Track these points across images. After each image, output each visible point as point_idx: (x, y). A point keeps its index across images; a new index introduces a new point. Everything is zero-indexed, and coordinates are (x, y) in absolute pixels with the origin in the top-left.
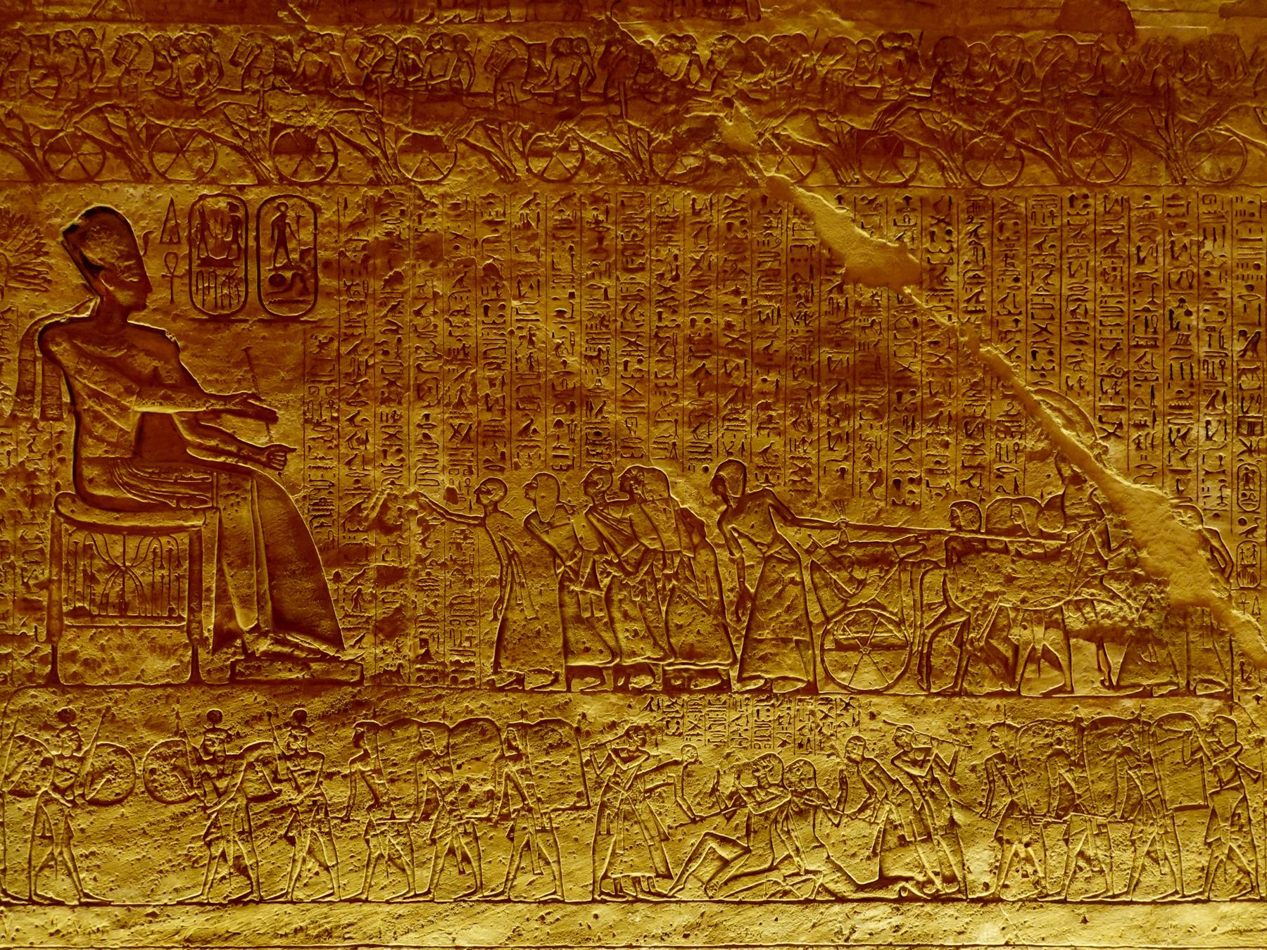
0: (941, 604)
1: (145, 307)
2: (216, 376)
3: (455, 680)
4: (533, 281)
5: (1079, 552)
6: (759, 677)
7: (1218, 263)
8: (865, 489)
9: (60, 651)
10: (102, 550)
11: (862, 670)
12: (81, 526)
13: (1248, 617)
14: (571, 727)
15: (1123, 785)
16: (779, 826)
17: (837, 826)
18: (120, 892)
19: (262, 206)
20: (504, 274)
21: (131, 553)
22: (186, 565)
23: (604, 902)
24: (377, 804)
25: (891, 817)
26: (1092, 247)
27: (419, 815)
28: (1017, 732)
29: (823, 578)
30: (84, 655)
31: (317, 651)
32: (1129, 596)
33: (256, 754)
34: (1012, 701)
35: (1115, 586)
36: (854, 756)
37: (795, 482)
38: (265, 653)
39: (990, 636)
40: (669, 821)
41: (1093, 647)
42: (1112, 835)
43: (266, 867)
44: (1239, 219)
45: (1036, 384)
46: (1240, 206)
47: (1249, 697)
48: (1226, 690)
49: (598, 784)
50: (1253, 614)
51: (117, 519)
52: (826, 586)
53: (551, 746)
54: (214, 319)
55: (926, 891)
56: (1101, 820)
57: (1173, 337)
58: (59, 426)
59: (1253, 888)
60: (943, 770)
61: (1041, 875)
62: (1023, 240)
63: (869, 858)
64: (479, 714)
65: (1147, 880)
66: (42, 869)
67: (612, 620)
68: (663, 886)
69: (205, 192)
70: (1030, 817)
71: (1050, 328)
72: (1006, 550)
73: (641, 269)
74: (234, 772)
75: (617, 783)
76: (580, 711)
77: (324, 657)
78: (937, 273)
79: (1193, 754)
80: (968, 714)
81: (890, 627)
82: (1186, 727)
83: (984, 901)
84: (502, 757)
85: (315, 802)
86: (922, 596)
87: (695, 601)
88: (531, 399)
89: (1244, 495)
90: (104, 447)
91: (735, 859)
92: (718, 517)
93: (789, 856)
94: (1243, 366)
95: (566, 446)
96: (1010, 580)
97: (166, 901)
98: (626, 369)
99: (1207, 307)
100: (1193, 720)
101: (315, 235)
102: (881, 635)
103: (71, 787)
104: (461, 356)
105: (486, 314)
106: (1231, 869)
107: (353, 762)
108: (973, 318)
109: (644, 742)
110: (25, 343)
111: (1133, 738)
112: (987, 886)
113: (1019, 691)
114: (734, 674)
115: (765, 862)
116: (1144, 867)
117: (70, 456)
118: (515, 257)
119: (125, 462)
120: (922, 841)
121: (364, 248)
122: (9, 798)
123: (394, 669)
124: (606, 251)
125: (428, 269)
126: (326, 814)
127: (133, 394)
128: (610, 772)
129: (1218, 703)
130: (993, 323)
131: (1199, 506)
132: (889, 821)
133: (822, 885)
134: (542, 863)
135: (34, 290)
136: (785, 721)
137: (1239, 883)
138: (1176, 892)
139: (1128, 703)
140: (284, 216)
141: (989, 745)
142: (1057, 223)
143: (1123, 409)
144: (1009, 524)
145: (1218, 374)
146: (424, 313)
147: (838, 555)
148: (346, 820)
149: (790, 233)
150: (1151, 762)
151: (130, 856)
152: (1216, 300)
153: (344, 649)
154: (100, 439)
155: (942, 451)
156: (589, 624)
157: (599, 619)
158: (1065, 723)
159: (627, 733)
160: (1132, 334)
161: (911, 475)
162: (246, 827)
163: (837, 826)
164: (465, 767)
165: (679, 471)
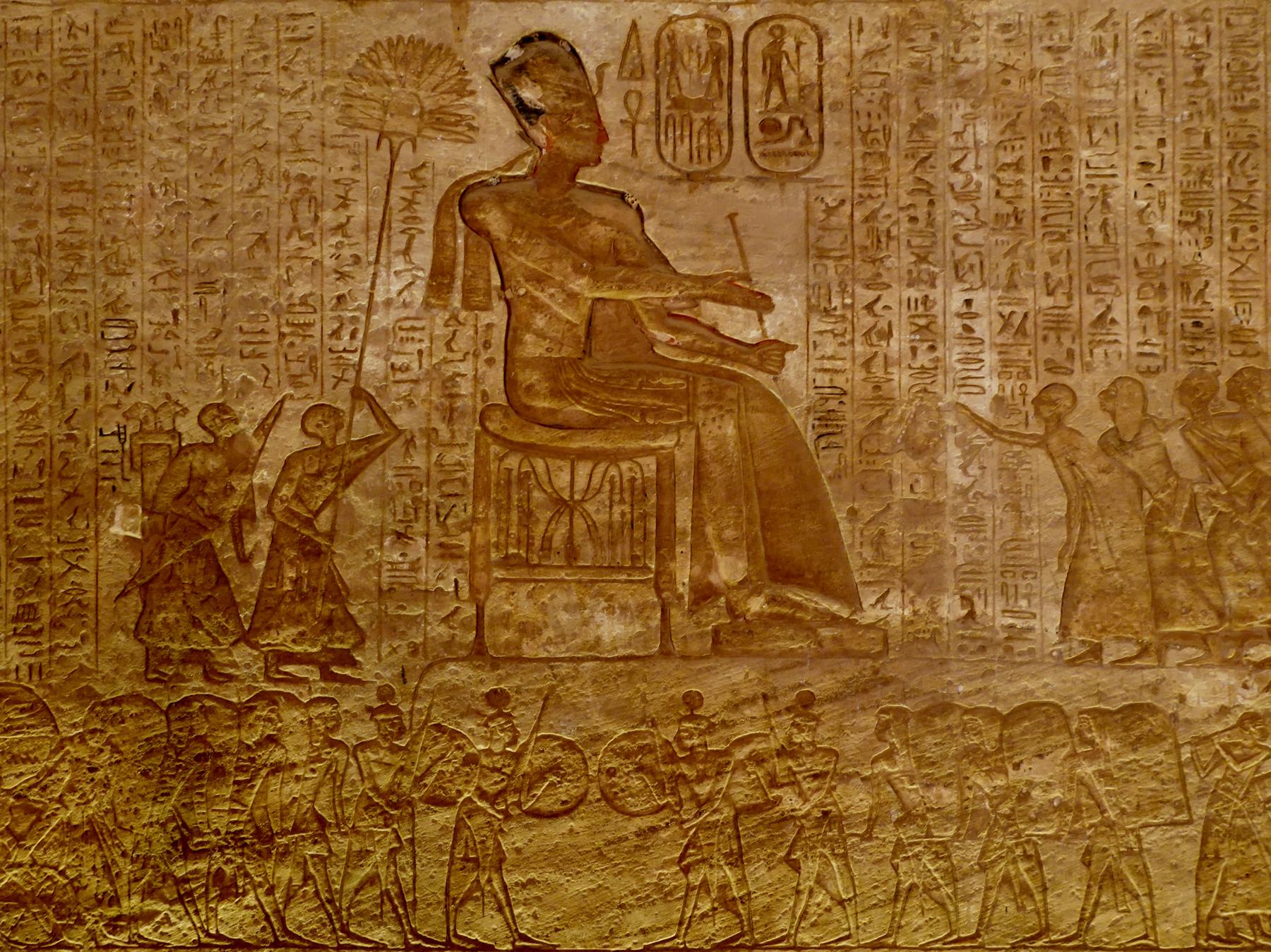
1: (599, 161)
2: (692, 250)
3: (1009, 650)
4: (1110, 124)
9: (487, 612)
10: (544, 478)
12: (514, 447)
18: (568, 933)
19: (751, 28)
20: (1072, 115)
21: (581, 483)
22: (653, 499)
24: (908, 817)
27: (963, 832)
30: (519, 617)
31: (826, 613)
33: (747, 750)
38: (760, 615)
43: (760, 901)
51: (563, 438)
53: (1139, 739)
54: (689, 177)
58: (485, 318)
64: (1041, 696)
66: (463, 902)
67: (1217, 572)
69: (678, 11)
74: (719, 773)
75: (1227, 790)
76: (1176, 692)
77: (835, 620)
84: (1074, 755)
85: (826, 814)
88: (1105, 280)
90: (546, 344)
95: (1154, 341)
97: (629, 945)
98: (1234, 238)
101: (820, 70)
103: (502, 792)
104: (1012, 223)
107: (874, 761)
110: (441, 210)
117: (500, 357)
118: (1085, 94)
119: (574, 363)
121: (883, 84)
122: (421, 806)
123: (927, 636)
124: (1206, 84)
125: (969, 110)
126: (841, 831)
127: (584, 274)
135: (457, 141)
140: (777, 43)
146: (963, 167)
148: (867, 836)
151: (581, 886)
153: (862, 610)
154: (541, 335)
156: (1189, 576)
157: (1204, 569)
159: (1241, 723)
162: (735, 847)
164: (1024, 766)
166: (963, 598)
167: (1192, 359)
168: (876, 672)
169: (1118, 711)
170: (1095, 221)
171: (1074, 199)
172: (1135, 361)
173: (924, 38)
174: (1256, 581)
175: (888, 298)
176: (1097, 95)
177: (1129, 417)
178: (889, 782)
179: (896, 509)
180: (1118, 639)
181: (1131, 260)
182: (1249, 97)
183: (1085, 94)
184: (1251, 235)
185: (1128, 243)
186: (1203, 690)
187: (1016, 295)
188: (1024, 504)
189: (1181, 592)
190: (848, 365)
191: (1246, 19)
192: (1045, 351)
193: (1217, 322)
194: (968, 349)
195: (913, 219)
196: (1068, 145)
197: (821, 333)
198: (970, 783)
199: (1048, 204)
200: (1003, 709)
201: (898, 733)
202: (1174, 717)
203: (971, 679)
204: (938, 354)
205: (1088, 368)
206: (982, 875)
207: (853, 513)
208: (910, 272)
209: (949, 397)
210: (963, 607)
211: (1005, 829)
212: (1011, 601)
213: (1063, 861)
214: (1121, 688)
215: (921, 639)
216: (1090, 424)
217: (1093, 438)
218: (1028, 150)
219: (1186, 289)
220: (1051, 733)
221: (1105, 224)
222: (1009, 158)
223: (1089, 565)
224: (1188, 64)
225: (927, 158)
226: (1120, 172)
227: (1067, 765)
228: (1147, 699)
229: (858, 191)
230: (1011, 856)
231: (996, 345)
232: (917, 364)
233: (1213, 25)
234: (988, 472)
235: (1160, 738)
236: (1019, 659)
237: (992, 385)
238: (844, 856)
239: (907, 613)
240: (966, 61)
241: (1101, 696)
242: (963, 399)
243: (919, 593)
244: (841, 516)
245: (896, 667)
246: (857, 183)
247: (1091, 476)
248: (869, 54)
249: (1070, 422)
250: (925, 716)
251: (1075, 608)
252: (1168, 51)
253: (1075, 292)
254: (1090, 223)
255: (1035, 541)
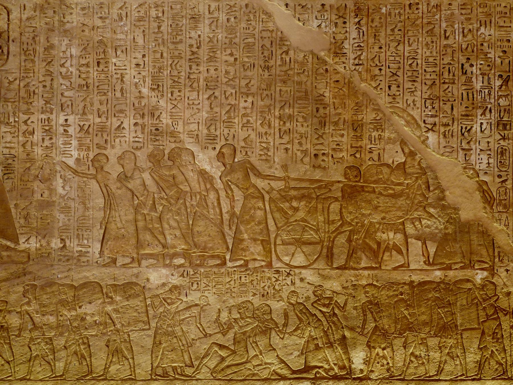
0: (339, 220)
3: (79, 260)
4: (124, 48)
5: (413, 193)
6: (241, 259)
7: (487, 38)
8: (299, 159)
11: (296, 255)
13: (502, 227)
14: (141, 286)
15: (435, 317)
16: (251, 339)
17: (282, 339)
20: (109, 45)
23: (156, 380)
25: (312, 334)
26: (421, 31)
27: (58, 333)
28: (379, 289)
29: (276, 207)
32: (439, 216)
34: (376, 272)
35: (432, 210)
36: (292, 302)
37: (261, 155)
39: (365, 237)
40: (193, 336)
41: (420, 243)
42: (429, 344)
44: (499, 16)
45: (391, 103)
46: (499, 9)
47: (502, 270)
48: (490, 266)
49: (155, 317)
50: (505, 225)
52: (277, 211)
53: (130, 296)
55: (330, 374)
56: (423, 336)
57: (463, 78)
59: (504, 373)
60: (340, 310)
61: (391, 365)
62: (384, 27)
63: (299, 356)
65: (448, 368)
68: (189, 371)
70: (385, 334)
71: (398, 73)
72: (374, 192)
73: (181, 42)
75: (165, 316)
76: (145, 277)
77: (8, 248)
78: (338, 44)
79: (472, 300)
80: (353, 279)
81: (312, 232)
82: (469, 285)
83: (360, 379)
84: (104, 302)
86: (329, 216)
87: (207, 218)
88: (121, 111)
89: (501, 162)
91: (228, 356)
92: (220, 174)
93: (257, 355)
94: (500, 93)
95: (140, 136)
96: (376, 208)
99: (482, 62)
100: (472, 282)
101: (8, 24)
102: (306, 236)
104: (85, 88)
105: (98, 66)
106: (493, 363)
107: (23, 305)
108: (357, 67)
109: (180, 293)
111: (441, 292)
112: (362, 371)
113: (380, 266)
114: (228, 257)
115: (244, 358)
116: (446, 362)
118: (115, 36)
120: (328, 347)
123: (46, 255)
124: (162, 32)
125: (68, 42)
128: (161, 310)
129: (485, 273)
130: (368, 71)
131: (477, 167)
132: (310, 336)
133: (274, 371)
134: (124, 359)
136: (255, 283)
137: (497, 369)
138: (463, 375)
139: (438, 273)
141: (364, 295)
142: (402, 18)
143: (436, 116)
144: (376, 178)
145: (487, 98)
146: (66, 65)
147: (284, 194)
148: (19, 336)
149: (261, 23)
150: (450, 304)
152: (486, 59)
155: (340, 139)
158: (405, 283)
159: (170, 290)
160: (441, 78)
161: (323, 152)
163: (282, 339)
164: (83, 307)
165: (200, 149)
166: (62, 239)
167: (155, 144)
168: (24, 269)
169: (122, 285)
170: (118, 88)
171: (110, 79)
172: (132, 144)
173: (50, 13)
174: (178, 233)
175: (33, 118)
176: (119, 36)
177: (129, 166)
178: (28, 314)
179: (34, 203)
180: (123, 256)
181: (132, 104)
182: (179, 38)
183: (115, 36)
184: (179, 94)
185: (131, 98)
186: (156, 276)
187: (86, 117)
188: (87, 202)
189: (148, 237)
190: (16, 145)
191: (179, 6)
192: (96, 141)
193: (165, 128)
194: (66, 139)
195: (44, 86)
196: (107, 57)
197: (5, 132)
198: (61, 314)
199: (99, 81)
200: (75, 284)
201: (32, 294)
202: (144, 287)
203: (63, 272)
204: (53, 141)
205: (113, 147)
206: (65, 351)
207: (16, 205)
208: (42, 108)
209: (58, 159)
210: (61, 243)
211: (74, 332)
212: (81, 241)
213: (98, 345)
214: (123, 276)
215: (43, 256)
216: (114, 169)
217: (115, 175)
218: (91, 59)
219: (153, 115)
220: (95, 294)
221: (122, 89)
222: (83, 62)
223: (112, 226)
224: (156, 25)
225: (51, 62)
226: (128, 68)
227: (101, 306)
228: (134, 280)
229: (22, 75)
230: (77, 343)
231: (77, 137)
232: (44, 145)
233: (166, 9)
234: (73, 188)
235: (138, 295)
236: (83, 264)
237: (75, 154)
238: (10, 343)
239: (38, 245)
240: (68, 22)
241: (115, 279)
242: (64, 159)
243: (44, 237)
244: (12, 206)
245: (32, 267)
246: (22, 71)
247: (114, 190)
248: (28, 19)
249: (106, 169)
250: (42, 288)
251: (106, 243)
252: (147, 19)
253: (110, 116)
254: (116, 88)
255: (91, 217)
